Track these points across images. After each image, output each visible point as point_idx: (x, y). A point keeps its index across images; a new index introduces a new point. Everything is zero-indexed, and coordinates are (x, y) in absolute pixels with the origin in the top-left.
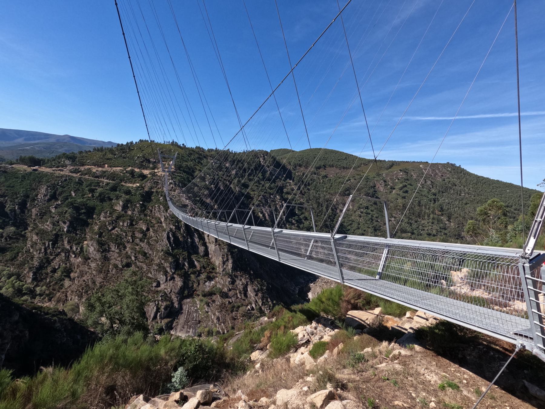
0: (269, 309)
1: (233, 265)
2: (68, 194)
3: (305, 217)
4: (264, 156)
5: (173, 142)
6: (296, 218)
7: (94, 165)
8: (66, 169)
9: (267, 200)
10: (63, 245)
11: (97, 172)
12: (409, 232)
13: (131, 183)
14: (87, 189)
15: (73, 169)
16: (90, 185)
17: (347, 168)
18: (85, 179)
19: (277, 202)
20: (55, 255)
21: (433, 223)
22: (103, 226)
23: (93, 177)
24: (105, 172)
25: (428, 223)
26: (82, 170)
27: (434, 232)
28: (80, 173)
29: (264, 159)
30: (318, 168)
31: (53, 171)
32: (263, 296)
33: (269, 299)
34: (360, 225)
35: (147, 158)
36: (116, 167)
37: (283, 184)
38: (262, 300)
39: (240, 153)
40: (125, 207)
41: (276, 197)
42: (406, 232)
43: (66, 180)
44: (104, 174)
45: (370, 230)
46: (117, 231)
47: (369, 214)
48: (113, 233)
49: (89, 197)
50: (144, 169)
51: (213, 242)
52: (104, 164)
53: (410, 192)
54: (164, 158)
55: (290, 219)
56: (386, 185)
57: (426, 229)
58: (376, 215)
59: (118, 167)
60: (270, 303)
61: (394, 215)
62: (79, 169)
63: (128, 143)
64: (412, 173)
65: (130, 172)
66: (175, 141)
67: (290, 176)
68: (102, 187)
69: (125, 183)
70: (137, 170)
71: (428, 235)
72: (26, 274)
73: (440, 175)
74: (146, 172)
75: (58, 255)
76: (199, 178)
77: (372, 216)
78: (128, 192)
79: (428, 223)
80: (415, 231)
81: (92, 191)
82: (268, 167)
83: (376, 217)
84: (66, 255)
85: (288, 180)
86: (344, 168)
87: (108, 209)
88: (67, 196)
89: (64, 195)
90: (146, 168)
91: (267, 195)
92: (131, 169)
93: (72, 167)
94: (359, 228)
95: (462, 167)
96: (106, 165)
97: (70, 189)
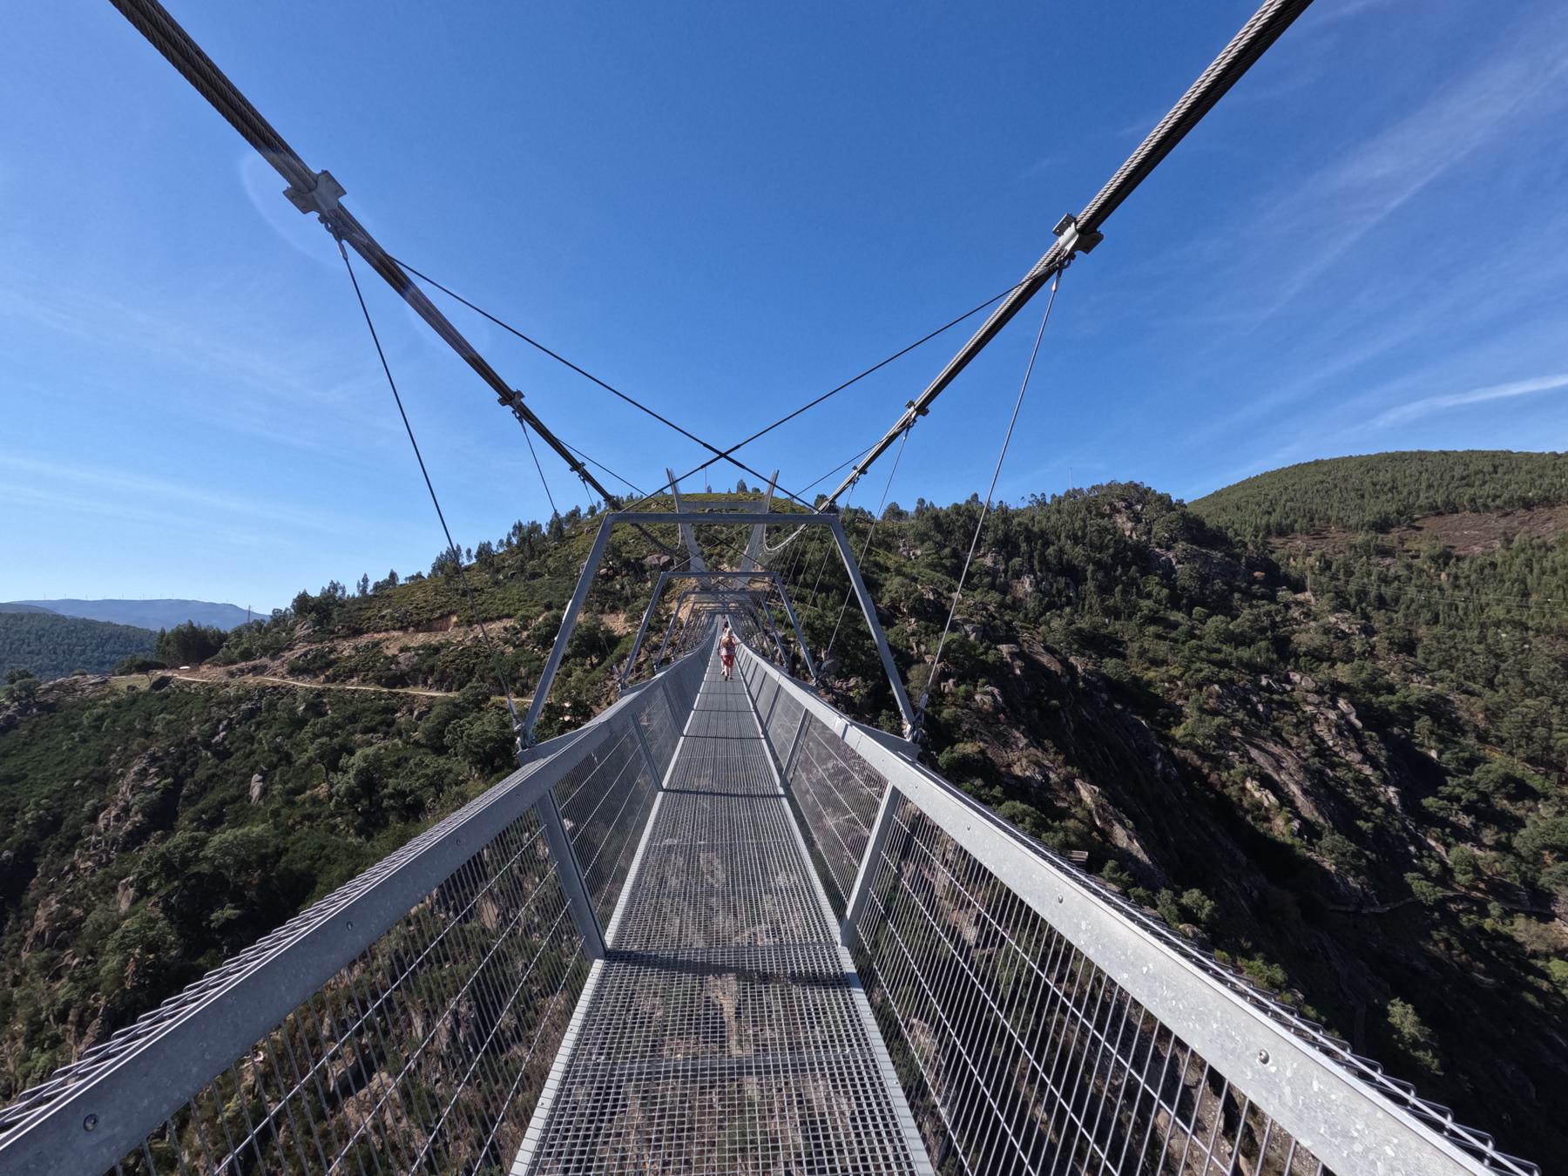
2: (233, 791)
3: (1508, 779)
4: (1129, 506)
6: (1453, 785)
8: (278, 662)
9: (1249, 701)
11: (402, 658)
14: (312, 751)
15: (305, 654)
17: (1548, 502)
18: (341, 700)
19: (1309, 709)
23: (379, 682)
24: (437, 650)
26: (346, 653)
28: (330, 672)
29: (1137, 519)
30: (1383, 526)
35: (632, 557)
36: (492, 620)
37: (1268, 614)
41: (1289, 681)
43: (252, 713)
44: (430, 661)
49: (315, 801)
50: (614, 610)
52: (445, 617)
54: (711, 541)
55: (1429, 802)
59: (499, 618)
62: (332, 650)
65: (544, 631)
67: (1276, 578)
68: (400, 734)
69: (520, 694)
76: (913, 611)
81: (332, 760)
82: (1169, 548)
85: (1284, 594)
86: (1528, 505)
88: (223, 803)
90: (612, 601)
91: (1243, 680)
92: (546, 619)
96: (454, 619)
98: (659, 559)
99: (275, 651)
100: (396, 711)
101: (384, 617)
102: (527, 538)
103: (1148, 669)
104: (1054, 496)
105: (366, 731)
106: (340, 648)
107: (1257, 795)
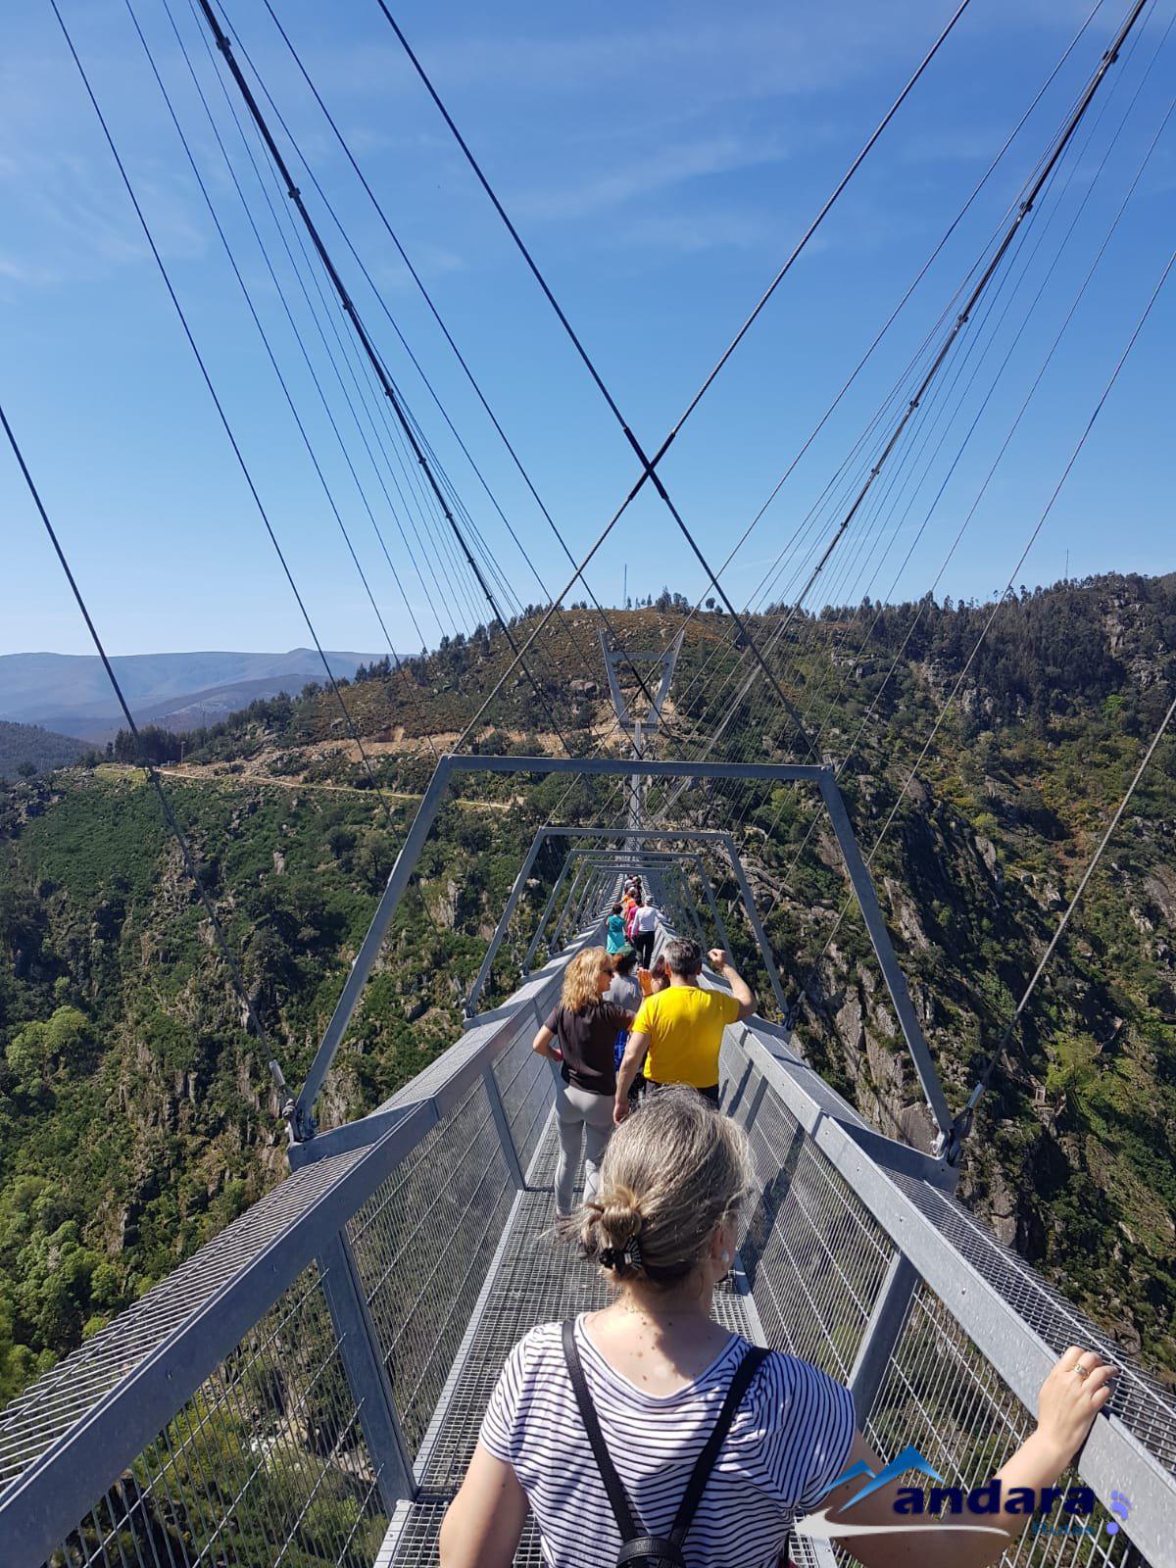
1: (1020, 1229)
2: (261, 866)
5: (667, 596)
7: (355, 733)
10: (233, 1087)
13: (491, 796)
15: (281, 758)
16: (339, 819)
20: (207, 1133)
22: (384, 999)
23: (350, 784)
31: (216, 773)
39: (989, 607)
40: (467, 907)
43: (254, 808)
46: (436, 1022)
48: (421, 1032)
51: (891, 1082)
59: (443, 732)
62: (301, 755)
63: (480, 630)
66: (672, 593)
69: (470, 798)
70: (516, 737)
72: (104, 1215)
74: (552, 744)
75: (217, 1129)
78: (477, 841)
84: (243, 1132)
87: (401, 922)
89: (250, 867)
93: (278, 753)
97: (269, 842)
98: (583, 684)
99: (249, 753)
100: (374, 809)
101: (336, 726)
102: (454, 653)
103: (1075, 800)
104: (1039, 588)
105: (355, 823)
106: (308, 754)
107: (1137, 921)
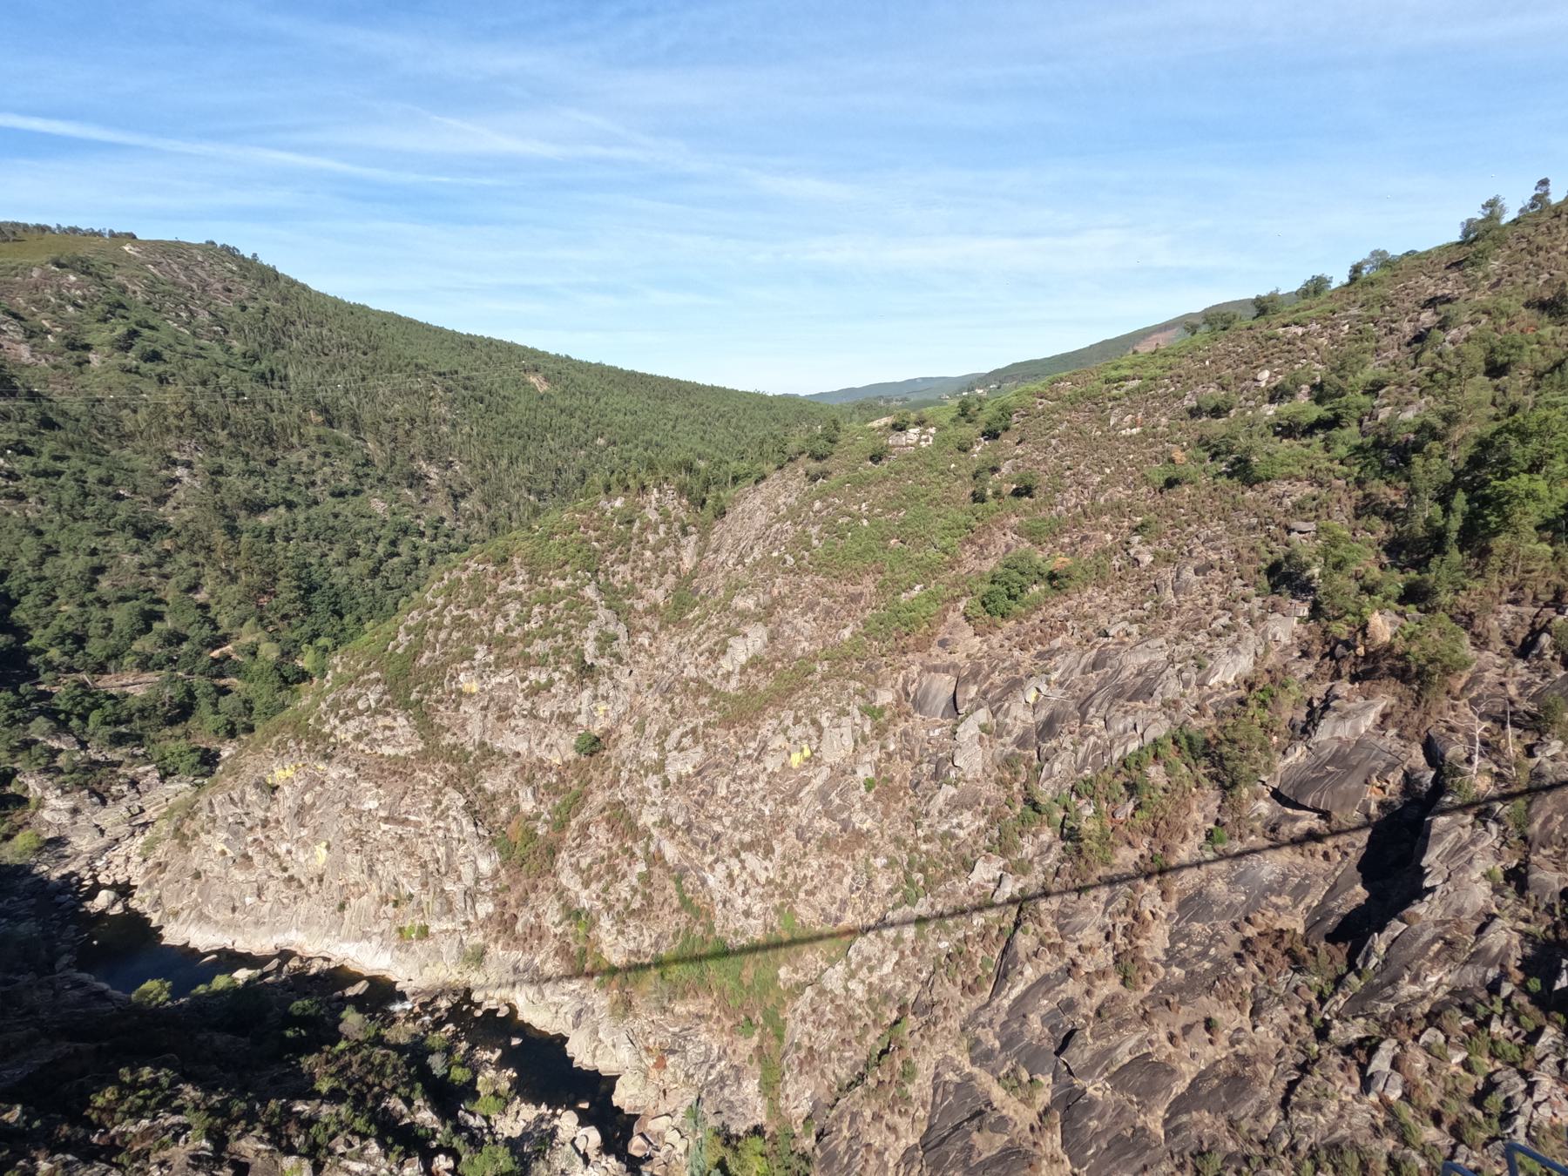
0: (364, 1137)
12: (276, 506)
21: (327, 455)
25: (312, 457)
27: (347, 481)
32: (268, 1128)
33: (299, 1107)
34: (48, 538)
38: (290, 1150)
42: (266, 508)
45: (116, 542)
47: (59, 474)
53: (166, 354)
56: (30, 334)
57: (318, 478)
58: (93, 475)
60: (326, 1110)
61: (175, 455)
64: (119, 279)
71: (333, 495)
73: (219, 286)
77: (82, 482)
79: (312, 457)
80: (290, 496)
83: (107, 481)
94: (51, 552)
95: (265, 259)
